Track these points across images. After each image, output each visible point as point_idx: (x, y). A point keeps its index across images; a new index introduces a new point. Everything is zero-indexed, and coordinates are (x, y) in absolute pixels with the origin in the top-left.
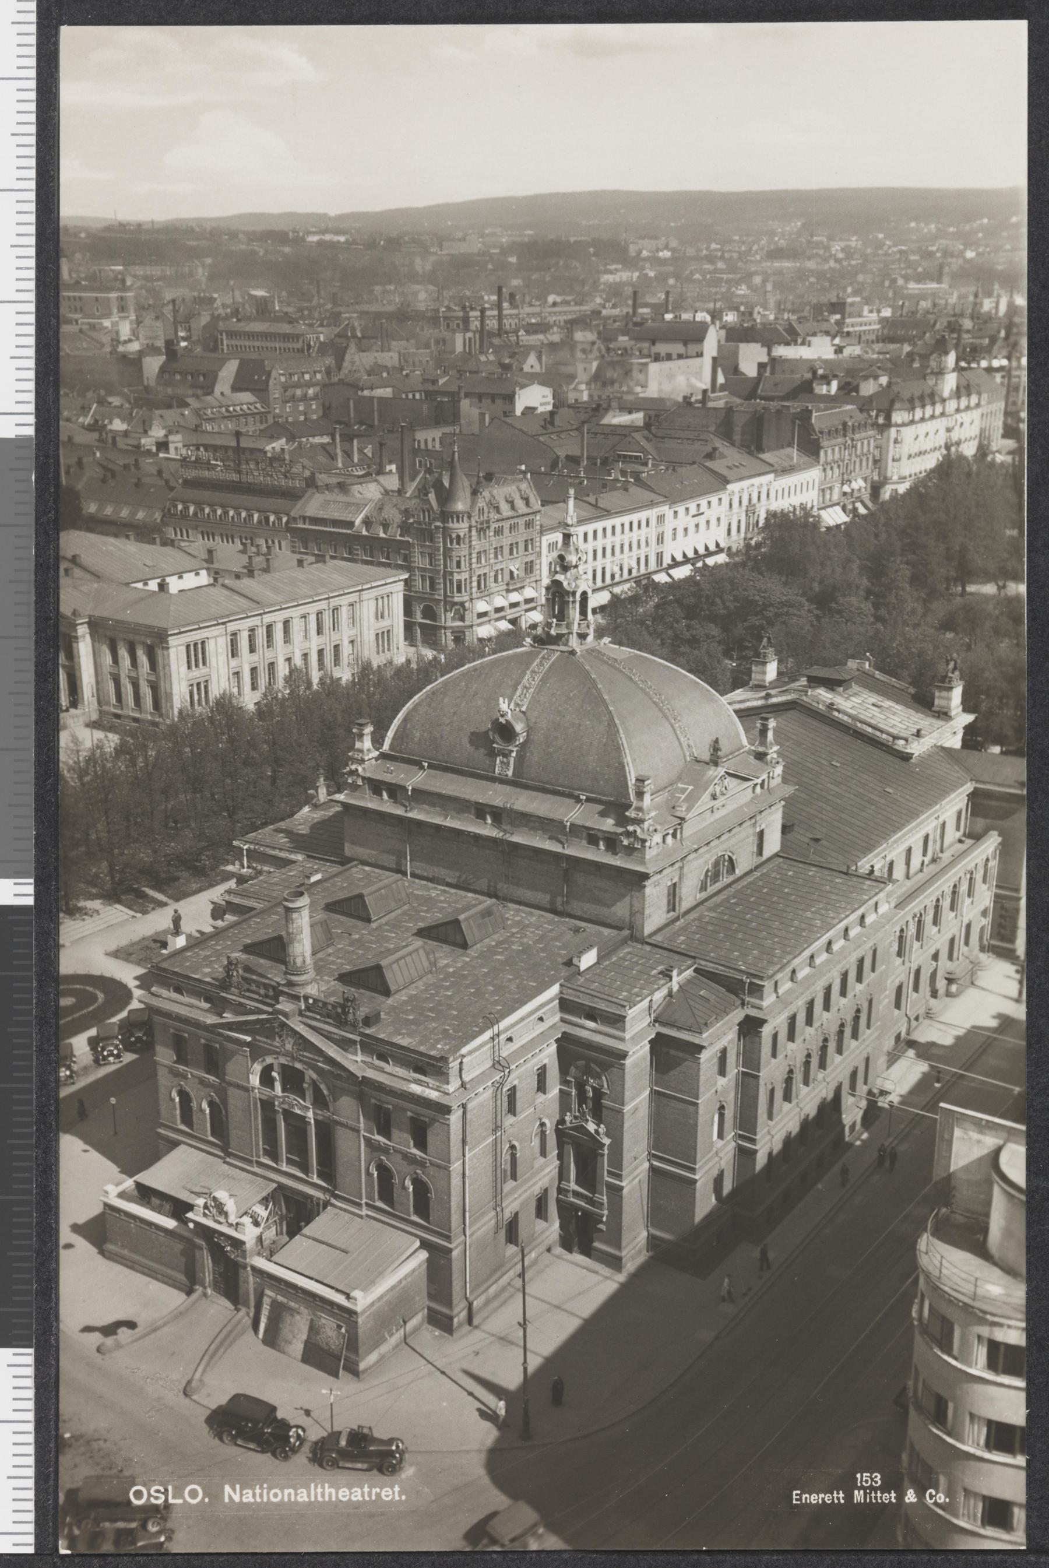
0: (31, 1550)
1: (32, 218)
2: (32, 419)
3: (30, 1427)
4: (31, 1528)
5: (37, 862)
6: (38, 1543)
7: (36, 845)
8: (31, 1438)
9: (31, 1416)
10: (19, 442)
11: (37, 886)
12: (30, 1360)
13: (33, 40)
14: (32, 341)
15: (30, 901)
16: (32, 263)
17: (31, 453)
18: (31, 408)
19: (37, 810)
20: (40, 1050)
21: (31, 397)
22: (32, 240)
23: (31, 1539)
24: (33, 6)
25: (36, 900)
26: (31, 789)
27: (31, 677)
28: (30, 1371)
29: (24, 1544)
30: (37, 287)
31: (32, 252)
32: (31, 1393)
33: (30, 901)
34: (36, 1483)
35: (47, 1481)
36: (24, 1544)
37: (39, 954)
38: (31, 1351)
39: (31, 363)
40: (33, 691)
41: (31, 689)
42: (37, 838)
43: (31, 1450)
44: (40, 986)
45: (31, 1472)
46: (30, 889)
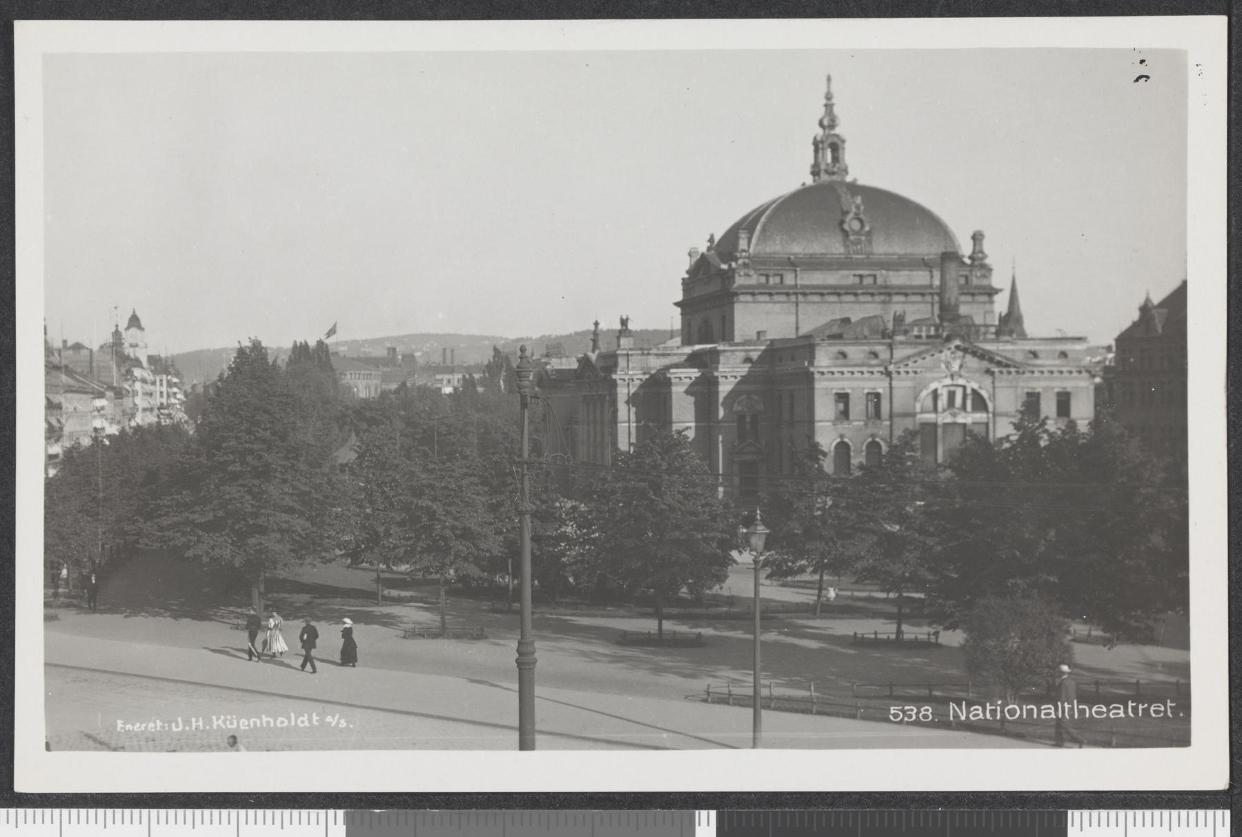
0: (1228, 813)
1: (171, 812)
2: (331, 812)
3: (1130, 813)
4: (1210, 813)
5: (681, 808)
6: (1225, 808)
7: (669, 808)
8: (1139, 813)
9: (1121, 813)
10: (349, 822)
11: (702, 808)
12: (1077, 813)
13: (30, 811)
14: (269, 812)
15: (713, 813)
16: (207, 812)
17: (358, 812)
18: (322, 812)
19: (641, 808)
20: (831, 805)
21: (313, 812)
22: (189, 812)
23: (1219, 812)
24: (4, 811)
25: (712, 809)
26: (624, 812)
27: (535, 812)
28: (1086, 813)
29: (1222, 818)
30: (226, 808)
31: (198, 812)
32: (1104, 813)
33: (713, 813)
34: (1174, 808)
35: (1173, 800)
36: (1222, 818)
37: (755, 806)
38: (1070, 812)
39: (287, 812)
40: (546, 811)
41: (545, 813)
42: (663, 808)
43: (1148, 813)
44: (781, 805)
45: (1166, 813)
46: (704, 813)
